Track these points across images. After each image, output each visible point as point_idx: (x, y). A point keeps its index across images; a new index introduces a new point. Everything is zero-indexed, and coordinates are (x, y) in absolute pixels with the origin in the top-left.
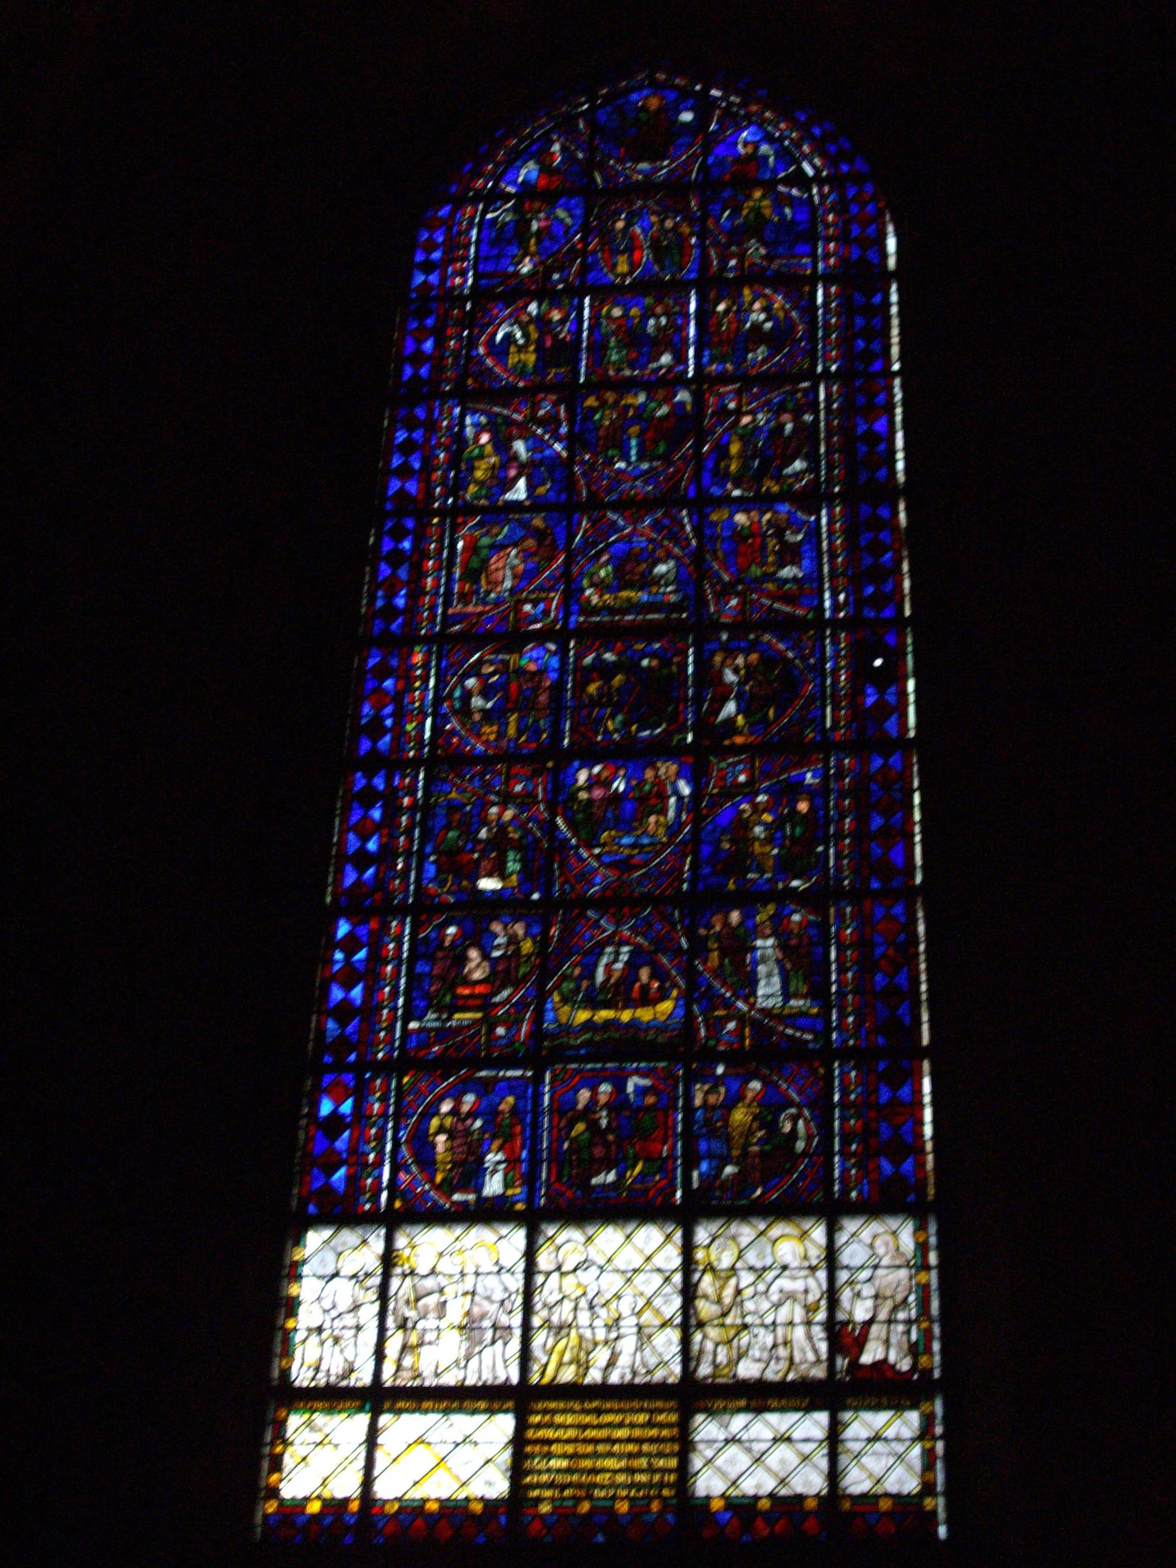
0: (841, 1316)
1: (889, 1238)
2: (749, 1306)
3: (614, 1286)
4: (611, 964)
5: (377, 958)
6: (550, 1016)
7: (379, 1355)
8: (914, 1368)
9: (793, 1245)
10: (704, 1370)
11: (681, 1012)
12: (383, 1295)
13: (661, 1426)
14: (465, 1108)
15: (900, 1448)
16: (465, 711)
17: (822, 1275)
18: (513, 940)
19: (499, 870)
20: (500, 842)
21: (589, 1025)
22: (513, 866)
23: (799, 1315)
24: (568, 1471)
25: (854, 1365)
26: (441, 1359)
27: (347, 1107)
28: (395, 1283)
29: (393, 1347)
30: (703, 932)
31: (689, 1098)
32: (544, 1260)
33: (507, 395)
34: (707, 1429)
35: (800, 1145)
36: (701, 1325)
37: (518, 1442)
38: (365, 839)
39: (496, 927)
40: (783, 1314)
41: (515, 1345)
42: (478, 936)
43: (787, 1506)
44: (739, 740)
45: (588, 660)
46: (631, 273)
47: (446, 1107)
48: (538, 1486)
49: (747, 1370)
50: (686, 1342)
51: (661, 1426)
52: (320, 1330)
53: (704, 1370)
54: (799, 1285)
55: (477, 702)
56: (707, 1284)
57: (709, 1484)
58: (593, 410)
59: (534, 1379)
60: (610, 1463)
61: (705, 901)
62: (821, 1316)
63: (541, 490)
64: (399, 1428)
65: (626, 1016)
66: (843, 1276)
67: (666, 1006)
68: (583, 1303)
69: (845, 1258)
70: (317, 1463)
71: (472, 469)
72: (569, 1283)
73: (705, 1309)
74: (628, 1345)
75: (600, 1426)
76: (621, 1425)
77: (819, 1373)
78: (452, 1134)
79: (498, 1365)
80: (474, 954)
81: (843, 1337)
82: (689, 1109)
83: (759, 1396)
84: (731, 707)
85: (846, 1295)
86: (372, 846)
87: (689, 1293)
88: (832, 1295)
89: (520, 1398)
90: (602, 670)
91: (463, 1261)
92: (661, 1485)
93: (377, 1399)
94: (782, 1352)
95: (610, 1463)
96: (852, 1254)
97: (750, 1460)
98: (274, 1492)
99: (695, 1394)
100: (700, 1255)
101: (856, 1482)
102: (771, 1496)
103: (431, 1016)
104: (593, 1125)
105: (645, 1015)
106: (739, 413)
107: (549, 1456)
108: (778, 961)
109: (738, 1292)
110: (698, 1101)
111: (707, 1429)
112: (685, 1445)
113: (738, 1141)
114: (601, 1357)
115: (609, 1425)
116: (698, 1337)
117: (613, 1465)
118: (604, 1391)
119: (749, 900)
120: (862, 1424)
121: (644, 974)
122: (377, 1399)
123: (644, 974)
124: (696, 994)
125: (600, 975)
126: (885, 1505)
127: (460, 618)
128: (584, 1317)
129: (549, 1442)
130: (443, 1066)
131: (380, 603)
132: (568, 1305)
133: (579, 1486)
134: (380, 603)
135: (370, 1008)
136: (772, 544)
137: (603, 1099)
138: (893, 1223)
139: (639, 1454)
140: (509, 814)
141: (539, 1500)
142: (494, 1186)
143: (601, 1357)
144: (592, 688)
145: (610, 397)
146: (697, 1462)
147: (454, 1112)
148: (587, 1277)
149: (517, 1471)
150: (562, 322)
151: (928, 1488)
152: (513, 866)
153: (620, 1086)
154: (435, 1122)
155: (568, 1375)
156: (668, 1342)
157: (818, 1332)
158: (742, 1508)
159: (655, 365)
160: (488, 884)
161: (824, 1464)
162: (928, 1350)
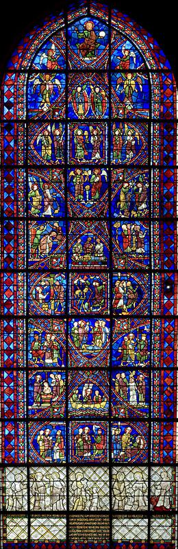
0: (152, 494)
1: (165, 473)
2: (128, 491)
3: (91, 487)
4: (87, 390)
5: (17, 385)
6: (69, 405)
7: (29, 503)
8: (170, 508)
9: (139, 474)
10: (116, 508)
11: (108, 405)
12: (28, 487)
13: (105, 522)
14: (47, 433)
15: (166, 528)
16: (37, 299)
17: (147, 483)
18: (57, 381)
19: (52, 357)
20: (51, 348)
21: (81, 409)
22: (56, 355)
23: (141, 493)
24: (82, 533)
25: (155, 507)
26: (46, 503)
27: (13, 432)
28: (31, 483)
29: (32, 501)
30: (114, 380)
31: (110, 432)
32: (72, 477)
33: (42, 168)
34: (116, 522)
35: (141, 447)
36: (115, 496)
37: (68, 525)
38: (9, 345)
39: (52, 376)
40: (136, 493)
41: (65, 501)
42: (46, 377)
43: (137, 543)
44: (124, 314)
45: (75, 282)
46: (84, 113)
47: (42, 432)
48: (74, 537)
49: (127, 508)
50: (111, 500)
51: (105, 522)
52: (12, 496)
53: (116, 508)
54: (141, 485)
55: (41, 296)
56: (116, 485)
57: (117, 537)
58: (73, 177)
59: (71, 509)
60: (92, 531)
61: (114, 369)
62: (147, 494)
63: (56, 211)
64: (35, 522)
65: (92, 406)
66: (152, 483)
67: (103, 404)
68: (83, 489)
69: (153, 478)
70: (16, 531)
71: (32, 201)
72: (79, 483)
73: (116, 492)
74: (95, 500)
75: (89, 522)
76: (94, 522)
77: (146, 508)
78: (44, 441)
79: (60, 506)
80: (46, 384)
81: (152, 499)
82: (111, 436)
83: (130, 514)
84: (121, 302)
85: (153, 489)
86: (11, 347)
87: (111, 488)
88: (149, 488)
89: (67, 514)
90: (82, 287)
91: (50, 479)
92: (105, 537)
93: (29, 514)
94: (136, 503)
95: (92, 531)
96: (155, 478)
97: (126, 530)
98: (5, 538)
99: (113, 514)
100: (114, 477)
101: (155, 536)
102: (133, 539)
103: (35, 405)
104: (84, 439)
105: (98, 406)
106: (123, 182)
107: (76, 529)
108: (136, 390)
109: (125, 487)
110: (113, 433)
111: (116, 522)
112: (111, 526)
113: (124, 445)
114: (89, 504)
115: (92, 521)
116: (114, 499)
117: (93, 534)
118: (90, 512)
119: (127, 369)
120: (156, 522)
121: (97, 392)
122: (29, 514)
123: (97, 392)
124: (113, 400)
125: (84, 394)
126: (162, 542)
127: (33, 263)
128: (83, 493)
129: (76, 525)
130: (40, 420)
131: (5, 256)
132: (79, 490)
133: (85, 537)
134: (5, 256)
135: (16, 403)
136: (135, 238)
137: (86, 432)
138: (166, 468)
139: (100, 529)
140: (53, 338)
141: (74, 540)
142: (57, 456)
143: (89, 504)
144: (77, 292)
145: (79, 171)
146: (114, 531)
147: (44, 434)
148: (84, 482)
149: (68, 533)
150: (60, 135)
151: (173, 538)
152: (56, 355)
153: (91, 427)
154: (39, 437)
155: (80, 508)
156: (106, 500)
157: (146, 498)
158: (127, 543)
159: (94, 158)
160: (48, 361)
161: (147, 532)
162: (175, 504)
